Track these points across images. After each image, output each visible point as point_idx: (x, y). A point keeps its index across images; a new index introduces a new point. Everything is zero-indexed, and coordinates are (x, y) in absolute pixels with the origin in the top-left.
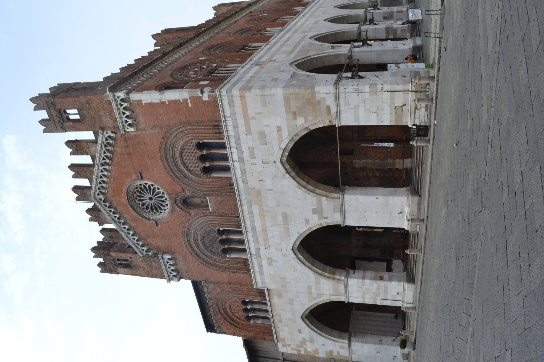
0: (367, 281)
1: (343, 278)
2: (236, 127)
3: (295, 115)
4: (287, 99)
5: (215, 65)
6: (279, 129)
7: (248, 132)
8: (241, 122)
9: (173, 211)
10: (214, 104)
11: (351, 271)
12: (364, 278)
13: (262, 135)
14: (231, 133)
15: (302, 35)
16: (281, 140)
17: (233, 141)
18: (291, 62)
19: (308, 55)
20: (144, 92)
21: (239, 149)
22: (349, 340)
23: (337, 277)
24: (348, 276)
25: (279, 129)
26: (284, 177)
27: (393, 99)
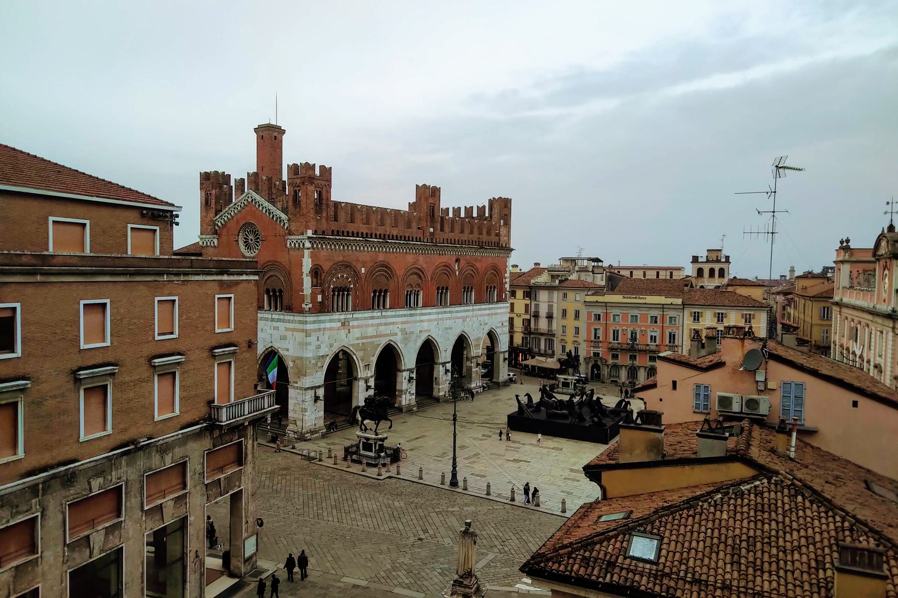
2: (289, 321)
4: (301, 358)
6: (287, 350)
7: (287, 329)
8: (291, 326)
10: (301, 312)
13: (283, 338)
14: (287, 317)
15: (397, 331)
16: (283, 349)
17: (282, 317)
21: (279, 320)
25: (287, 350)
27: (299, 419)
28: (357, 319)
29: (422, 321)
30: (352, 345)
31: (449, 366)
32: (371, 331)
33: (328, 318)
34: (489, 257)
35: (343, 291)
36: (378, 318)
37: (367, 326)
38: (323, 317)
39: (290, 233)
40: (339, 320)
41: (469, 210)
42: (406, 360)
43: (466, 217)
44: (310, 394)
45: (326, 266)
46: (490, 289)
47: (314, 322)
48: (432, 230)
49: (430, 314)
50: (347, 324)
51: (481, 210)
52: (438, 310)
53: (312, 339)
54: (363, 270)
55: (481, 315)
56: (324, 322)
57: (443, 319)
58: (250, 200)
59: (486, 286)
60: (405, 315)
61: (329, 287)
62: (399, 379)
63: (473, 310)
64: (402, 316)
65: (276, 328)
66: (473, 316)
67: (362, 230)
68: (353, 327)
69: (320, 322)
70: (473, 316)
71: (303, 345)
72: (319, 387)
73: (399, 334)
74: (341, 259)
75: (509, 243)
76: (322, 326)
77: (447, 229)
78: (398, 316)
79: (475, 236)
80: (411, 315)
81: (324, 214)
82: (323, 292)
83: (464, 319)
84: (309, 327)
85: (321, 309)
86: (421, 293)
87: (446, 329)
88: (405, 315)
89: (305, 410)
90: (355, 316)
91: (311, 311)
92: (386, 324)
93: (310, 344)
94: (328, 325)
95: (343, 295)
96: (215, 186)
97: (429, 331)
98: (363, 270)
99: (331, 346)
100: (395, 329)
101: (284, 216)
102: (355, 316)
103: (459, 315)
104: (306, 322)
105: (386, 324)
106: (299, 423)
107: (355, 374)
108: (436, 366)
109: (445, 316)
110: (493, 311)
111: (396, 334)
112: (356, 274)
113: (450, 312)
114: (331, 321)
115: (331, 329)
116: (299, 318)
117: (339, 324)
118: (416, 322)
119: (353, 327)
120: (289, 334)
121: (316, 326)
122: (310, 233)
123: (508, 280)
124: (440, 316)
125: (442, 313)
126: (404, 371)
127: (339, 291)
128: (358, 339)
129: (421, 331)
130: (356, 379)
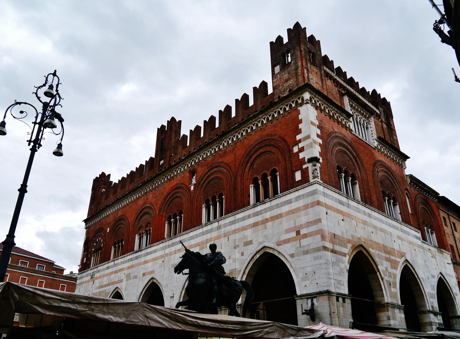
28: (99, 271)
29: (146, 262)
32: (105, 281)
36: (112, 267)
37: (104, 276)
49: (155, 251)
52: (164, 244)
55: (235, 232)
57: (170, 254)
60: (131, 260)
63: (219, 228)
80: (137, 258)
88: (131, 260)
92: (116, 272)
97: (153, 272)
102: (99, 268)
105: (116, 272)
110: (268, 215)
111: (122, 281)
118: (140, 264)
124: (167, 251)
125: (169, 246)
128: (97, 288)
129: (144, 274)
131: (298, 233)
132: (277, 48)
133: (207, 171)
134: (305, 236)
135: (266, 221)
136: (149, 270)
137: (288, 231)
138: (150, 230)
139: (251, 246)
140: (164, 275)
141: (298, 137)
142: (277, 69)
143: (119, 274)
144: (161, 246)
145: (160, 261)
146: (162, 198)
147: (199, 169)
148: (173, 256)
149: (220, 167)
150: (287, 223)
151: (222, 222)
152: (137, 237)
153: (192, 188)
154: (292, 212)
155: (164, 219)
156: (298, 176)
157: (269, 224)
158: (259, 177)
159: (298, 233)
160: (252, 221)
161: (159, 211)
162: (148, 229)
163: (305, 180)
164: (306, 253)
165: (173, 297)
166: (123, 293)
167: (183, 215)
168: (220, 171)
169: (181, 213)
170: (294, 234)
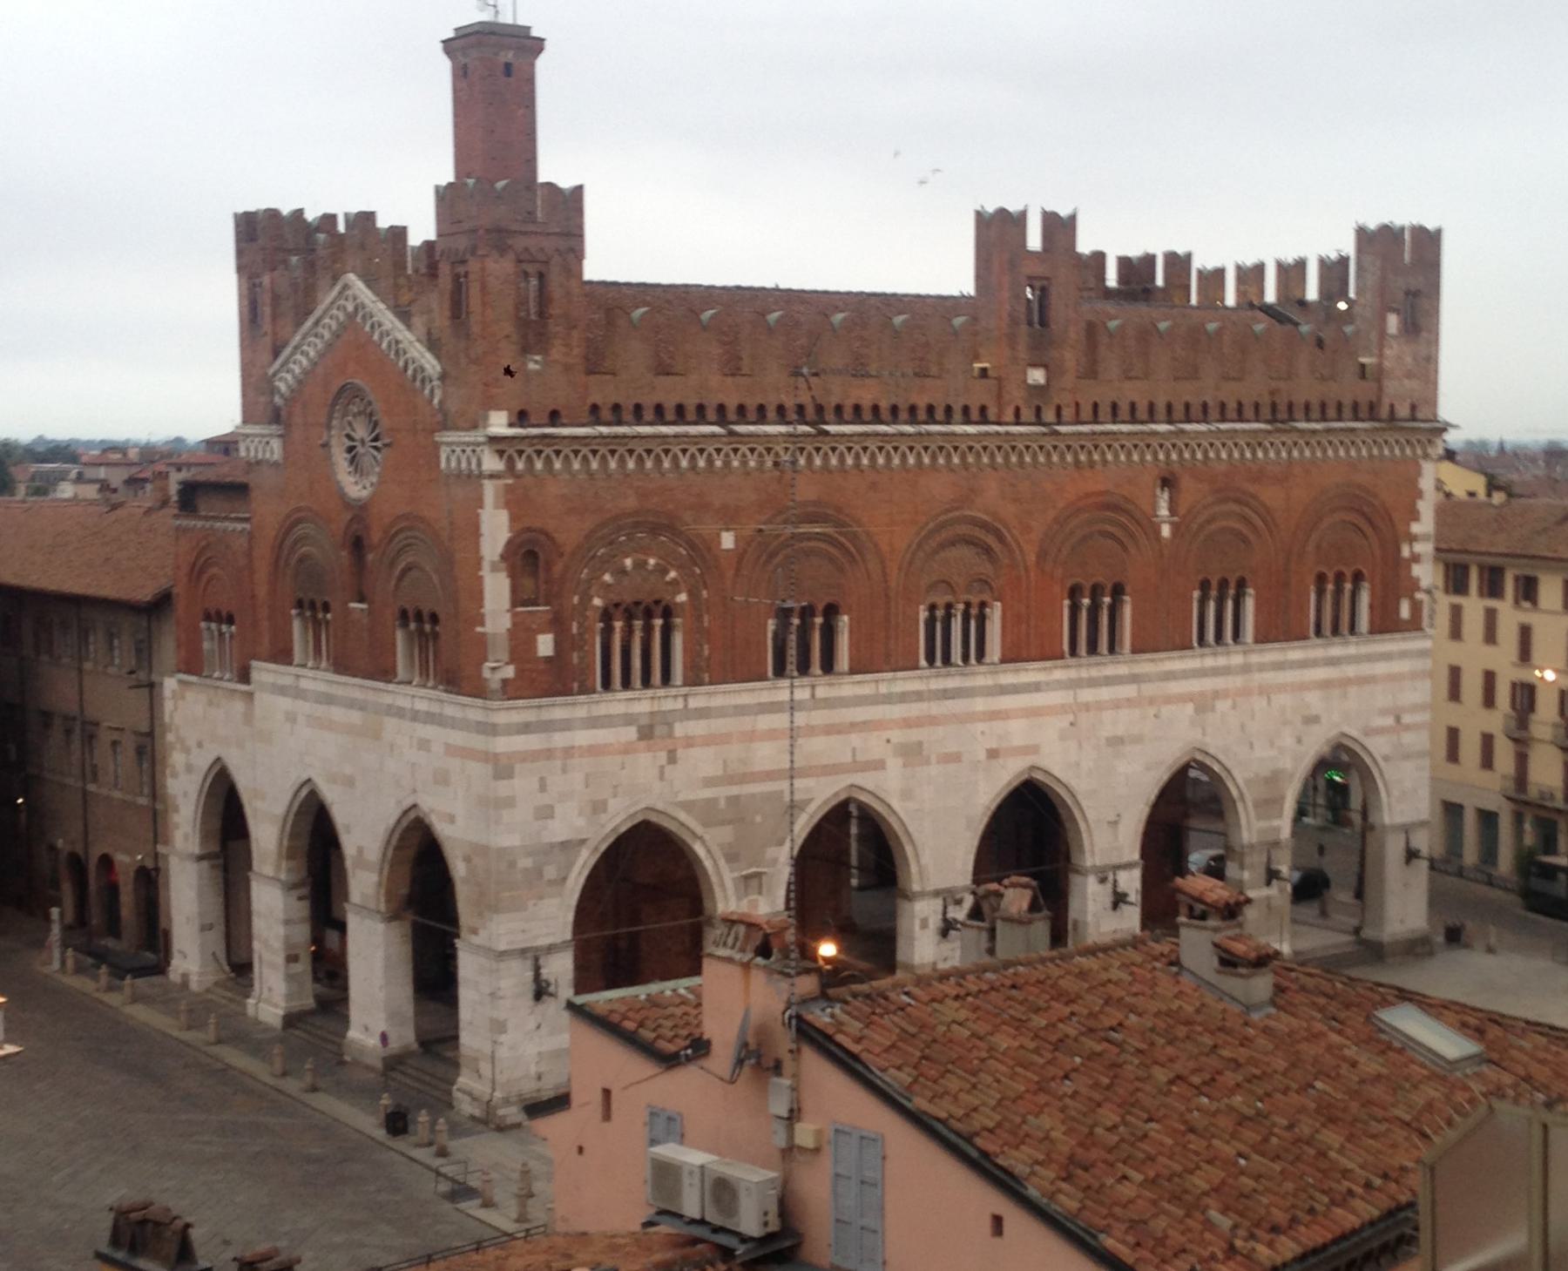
0: (281, 930)
1: (283, 876)
3: (467, 859)
5: (682, 597)
7: (451, 750)
9: (346, 503)
10: (479, 691)
11: (305, 891)
12: (287, 922)
13: (442, 779)
18: (660, 806)
19: (699, 830)
20: (503, 517)
22: (200, 858)
23: (284, 864)
24: (290, 887)
25: (452, 819)
26: (399, 802)
28: (703, 713)
30: (688, 806)
31: (1131, 882)
33: (581, 712)
34: (1337, 454)
35: (648, 615)
37: (751, 736)
38: (559, 709)
39: (445, 426)
40: (628, 719)
41: (1292, 273)
42: (926, 859)
43: (1239, 306)
44: (517, 977)
45: (569, 532)
46: (1338, 582)
47: (526, 728)
48: (1037, 376)
49: (1036, 687)
50: (660, 730)
51: (1334, 271)
52: (1072, 674)
53: (522, 785)
54: (728, 541)
55: (1282, 688)
56: (566, 725)
57: (1100, 706)
58: (350, 308)
59: (1331, 574)
60: (918, 696)
61: (586, 599)
62: (903, 925)
64: (904, 698)
65: (424, 745)
66: (1246, 692)
67: (720, 398)
68: (690, 742)
69: (547, 727)
70: (1246, 692)
71: (494, 806)
72: (551, 949)
73: (894, 764)
74: (631, 503)
75: (1432, 402)
76: (559, 740)
77: (1111, 365)
78: (888, 699)
79: (1254, 387)
81: (557, 353)
82: (557, 624)
83: (1203, 704)
84: (503, 744)
85: (553, 680)
86: (995, 614)
87: (1116, 742)
88: (918, 696)
89: (499, 1027)
90: (694, 703)
91: (510, 691)
92: (830, 730)
93: (510, 802)
94: (582, 738)
95: (648, 630)
96: (284, 258)
97: (1034, 749)
98: (728, 541)
99: (598, 807)
100: (873, 746)
101: (431, 364)
103: (1175, 687)
104: (492, 730)
105: (830, 730)
106: (485, 1068)
107: (707, 904)
108: (1075, 879)
109: (1105, 693)
110: (1350, 671)
112: (701, 552)
113: (1135, 679)
114: (593, 723)
115: (594, 751)
116: (473, 710)
117: (631, 733)
118: (972, 717)
119: (690, 742)
120: (454, 764)
121: (533, 742)
122: (499, 423)
123: (1425, 548)
124: (1087, 695)
125: (1093, 683)
126: (923, 895)
127: (629, 617)
128: (709, 782)
129: (993, 754)
130: (909, 897)
131: (1398, 719)
132: (1379, 243)
133: (1210, 499)
134: (1408, 728)
135: (1345, 683)
136: (1017, 741)
137: (1384, 712)
138: (983, 605)
139: (1315, 728)
140: (1078, 764)
141: (1416, 528)
142: (1393, 322)
143: (855, 739)
144: (1059, 673)
145: (1063, 722)
146: (1051, 514)
147: (1186, 483)
148: (1107, 715)
149: (1247, 505)
150: (1382, 697)
151: (1255, 658)
152: (923, 614)
153: (1166, 531)
154: (1392, 678)
155: (1057, 589)
156: (1405, 611)
157: (1353, 691)
158: (1331, 576)
159: (1398, 719)
160: (1321, 673)
161: (1038, 557)
162: (975, 600)
163: (1415, 625)
164: (1407, 757)
165: (1114, 824)
166: (896, 805)
167: (1127, 598)
168: (1246, 520)
169: (1118, 591)
170: (1389, 721)
